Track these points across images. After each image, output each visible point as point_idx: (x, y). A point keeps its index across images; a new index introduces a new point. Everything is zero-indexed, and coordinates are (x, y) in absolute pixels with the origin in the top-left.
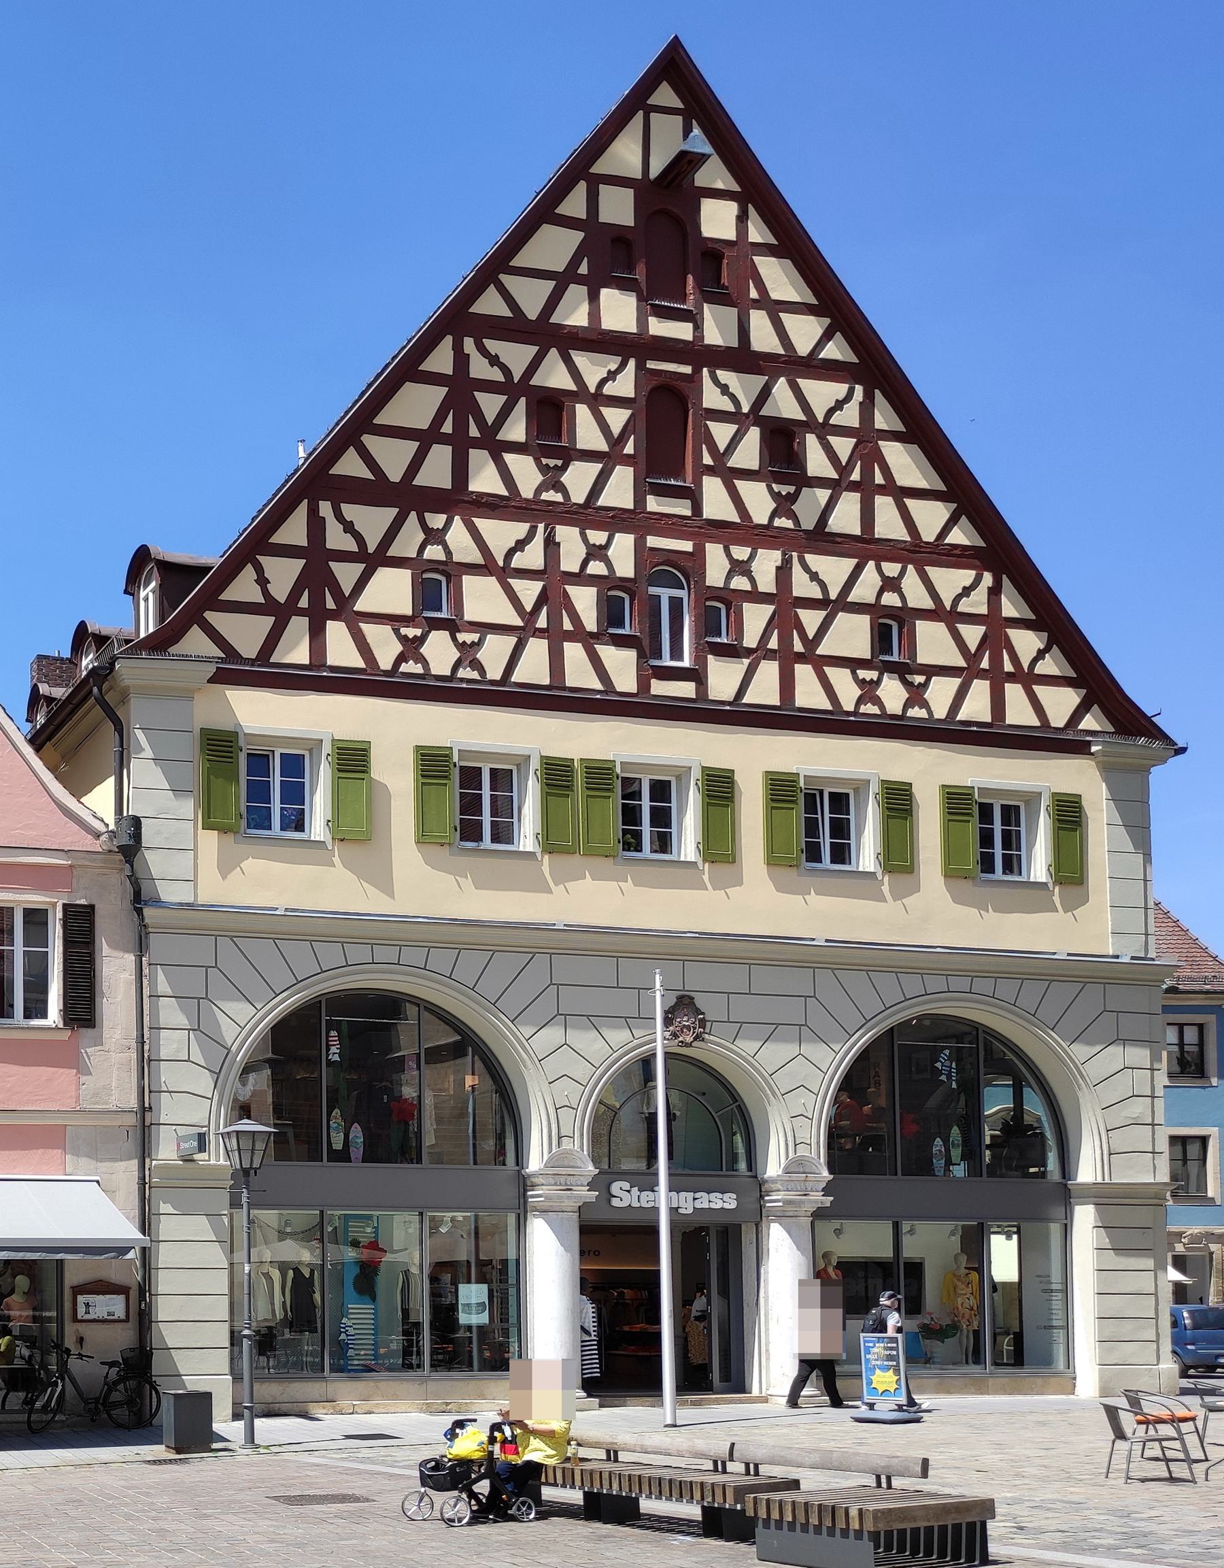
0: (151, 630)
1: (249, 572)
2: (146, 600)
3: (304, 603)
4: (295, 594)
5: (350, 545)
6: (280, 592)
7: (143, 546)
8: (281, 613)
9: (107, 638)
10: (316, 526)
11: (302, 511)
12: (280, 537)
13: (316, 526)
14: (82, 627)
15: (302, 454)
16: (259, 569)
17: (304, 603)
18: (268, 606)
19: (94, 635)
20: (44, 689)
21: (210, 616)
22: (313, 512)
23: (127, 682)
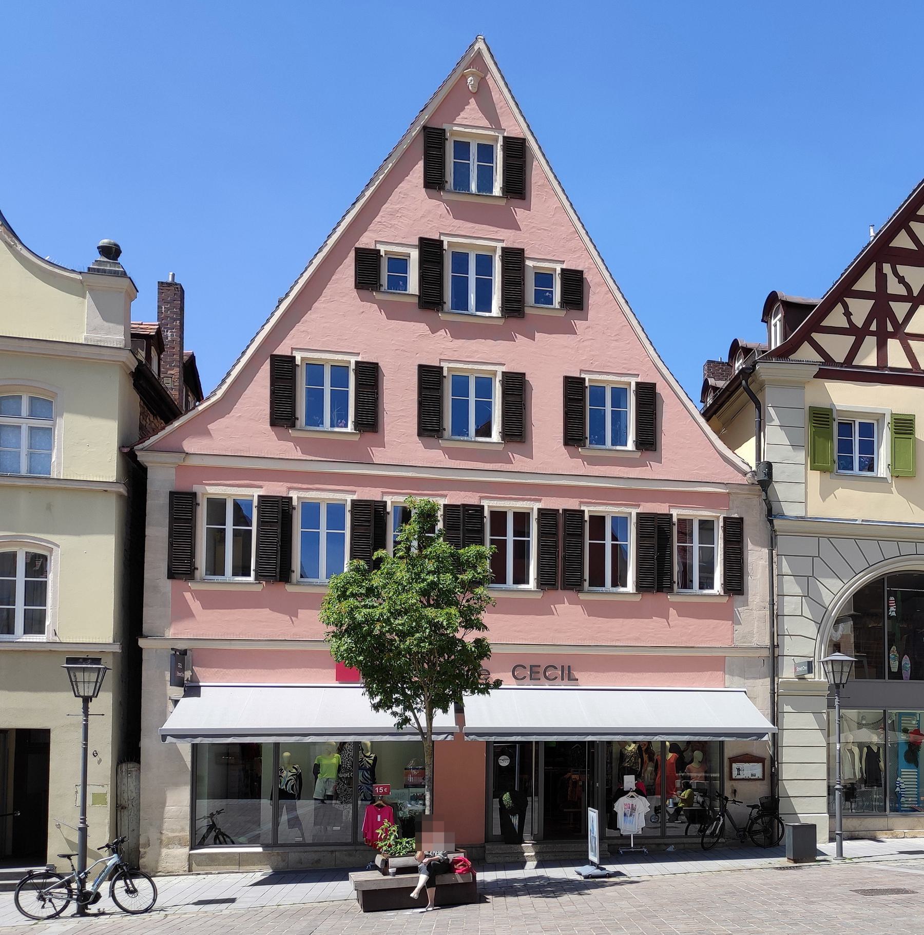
0: (778, 344)
1: (839, 308)
2: (775, 325)
3: (873, 327)
4: (868, 322)
5: (903, 291)
6: (859, 321)
7: (773, 292)
8: (859, 334)
9: (751, 350)
10: (881, 279)
11: (872, 269)
12: (858, 286)
13: (881, 279)
14: (735, 342)
15: (872, 234)
16: (846, 307)
17: (873, 327)
18: (852, 330)
19: (743, 348)
20: (711, 382)
21: (816, 336)
22: (879, 270)
23: (763, 378)
